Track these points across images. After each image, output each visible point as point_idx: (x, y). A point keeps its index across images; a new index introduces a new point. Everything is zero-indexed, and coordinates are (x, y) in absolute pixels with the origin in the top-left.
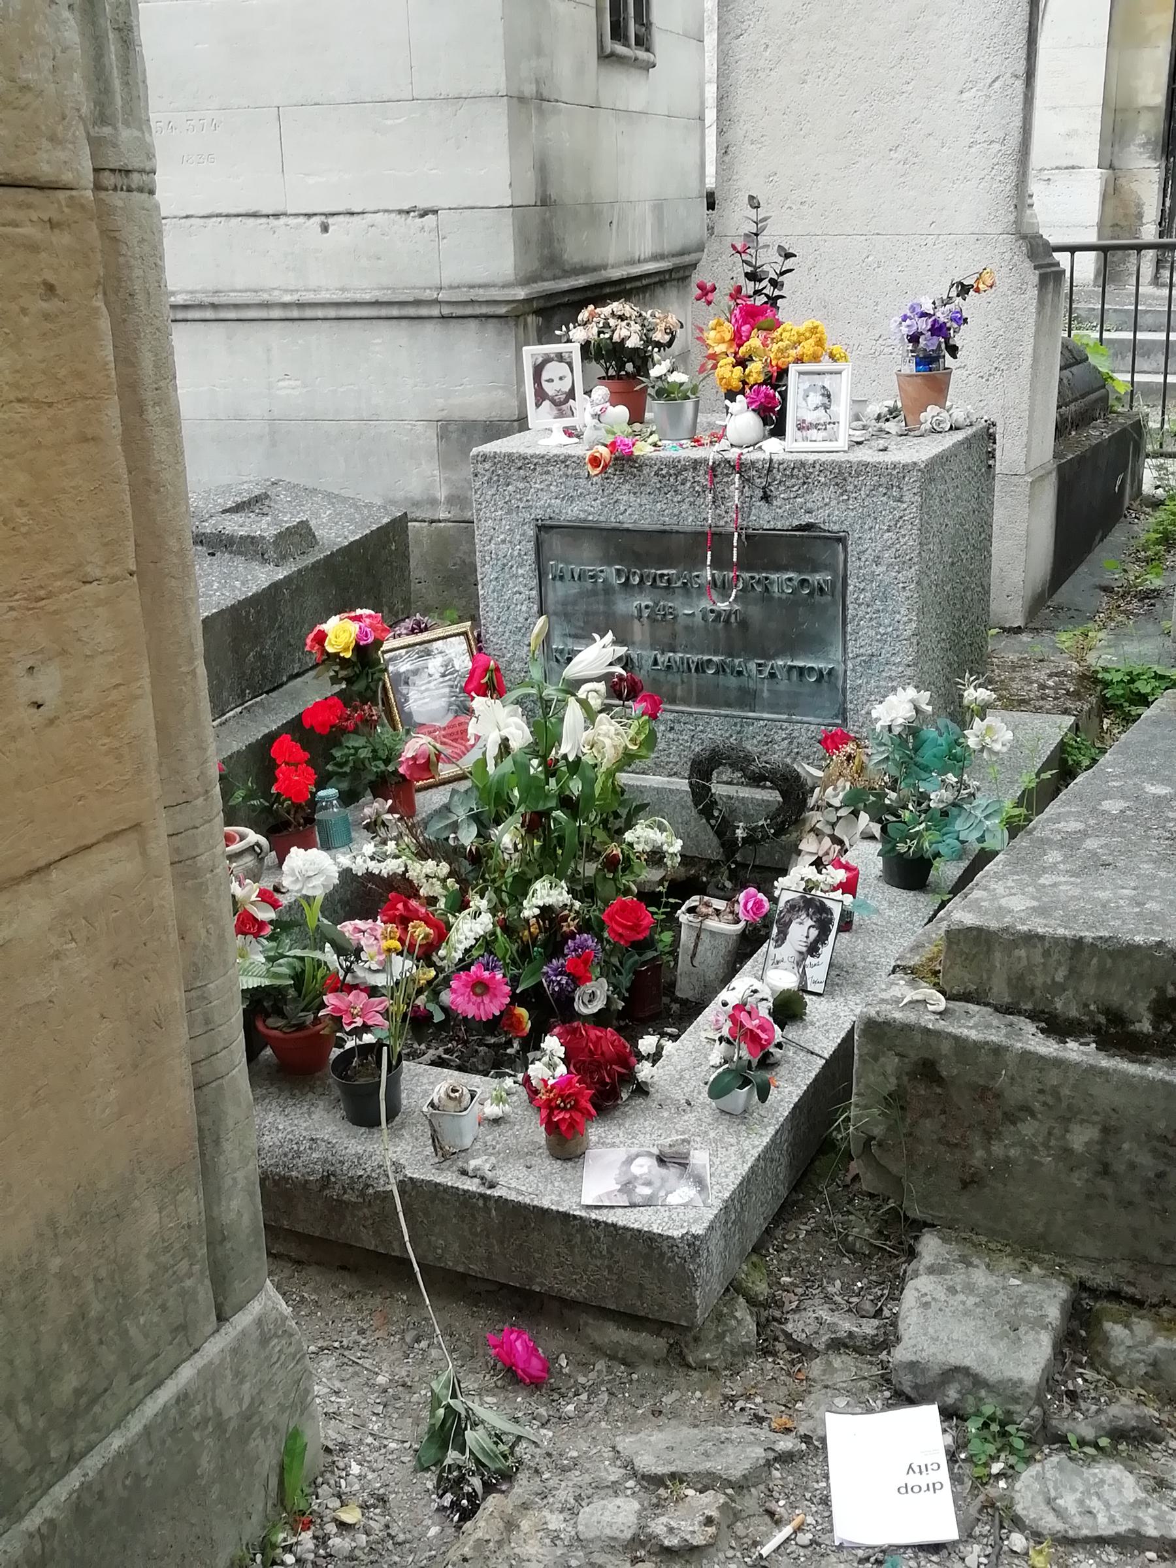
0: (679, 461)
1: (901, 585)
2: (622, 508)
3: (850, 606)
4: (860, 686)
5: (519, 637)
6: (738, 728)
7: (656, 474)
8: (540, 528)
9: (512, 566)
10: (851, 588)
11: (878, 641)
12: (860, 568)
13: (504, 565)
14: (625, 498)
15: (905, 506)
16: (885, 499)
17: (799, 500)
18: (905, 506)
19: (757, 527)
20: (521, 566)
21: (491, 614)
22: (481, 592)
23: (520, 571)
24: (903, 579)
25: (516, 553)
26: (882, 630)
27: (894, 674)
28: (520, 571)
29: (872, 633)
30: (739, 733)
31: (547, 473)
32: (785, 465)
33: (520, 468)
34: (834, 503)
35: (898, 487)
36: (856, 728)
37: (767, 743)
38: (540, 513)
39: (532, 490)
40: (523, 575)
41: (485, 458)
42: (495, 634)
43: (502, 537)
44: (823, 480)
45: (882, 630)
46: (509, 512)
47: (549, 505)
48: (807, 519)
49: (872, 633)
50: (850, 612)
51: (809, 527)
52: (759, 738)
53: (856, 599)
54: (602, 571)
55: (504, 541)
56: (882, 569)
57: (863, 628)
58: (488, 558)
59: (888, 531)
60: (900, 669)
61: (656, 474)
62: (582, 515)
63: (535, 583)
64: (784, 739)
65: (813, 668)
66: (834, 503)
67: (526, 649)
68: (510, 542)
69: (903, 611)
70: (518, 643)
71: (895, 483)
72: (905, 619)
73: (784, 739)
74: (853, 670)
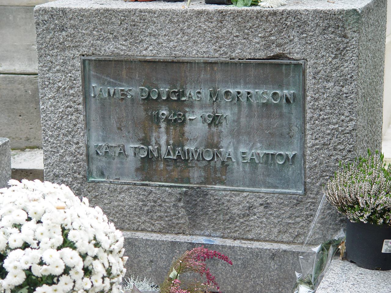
0: (186, 12)
1: (345, 95)
2: (145, 46)
3: (309, 111)
4: (315, 166)
5: (70, 138)
6: (227, 198)
7: (171, 21)
8: (84, 62)
9: (65, 88)
10: (308, 98)
11: (329, 134)
12: (314, 84)
13: (60, 87)
14: (148, 39)
15: (348, 40)
16: (333, 36)
17: (272, 38)
18: (348, 40)
19: (242, 57)
20: (71, 88)
21: (49, 123)
22: (42, 107)
23: (71, 92)
24: (346, 91)
25: (68, 79)
26: (331, 127)
27: (339, 157)
28: (71, 92)
29: (323, 129)
30: (229, 201)
31: (89, 22)
32: (262, 14)
33: (70, 19)
34: (296, 39)
35: (343, 27)
36: (312, 196)
37: (249, 208)
38: (84, 50)
39: (80, 35)
40: (73, 95)
41: (45, 11)
42: (52, 136)
43: (58, 67)
44: (289, 23)
45: (331, 127)
46: (64, 50)
47: (92, 45)
48: (277, 51)
49: (323, 129)
50: (308, 115)
51: (277, 57)
52: (243, 205)
53: (313, 105)
54: (130, 90)
55: (58, 71)
56: (331, 84)
57: (317, 125)
58: (47, 83)
59: (335, 58)
60: (344, 153)
61: (171, 21)
62: (116, 51)
63: (81, 100)
64: (261, 205)
65: (280, 155)
66: (296, 39)
67: (75, 146)
68: (63, 71)
69: (346, 114)
70: (68, 142)
71: (341, 24)
72: (348, 119)
73: (261, 205)
74: (311, 155)
